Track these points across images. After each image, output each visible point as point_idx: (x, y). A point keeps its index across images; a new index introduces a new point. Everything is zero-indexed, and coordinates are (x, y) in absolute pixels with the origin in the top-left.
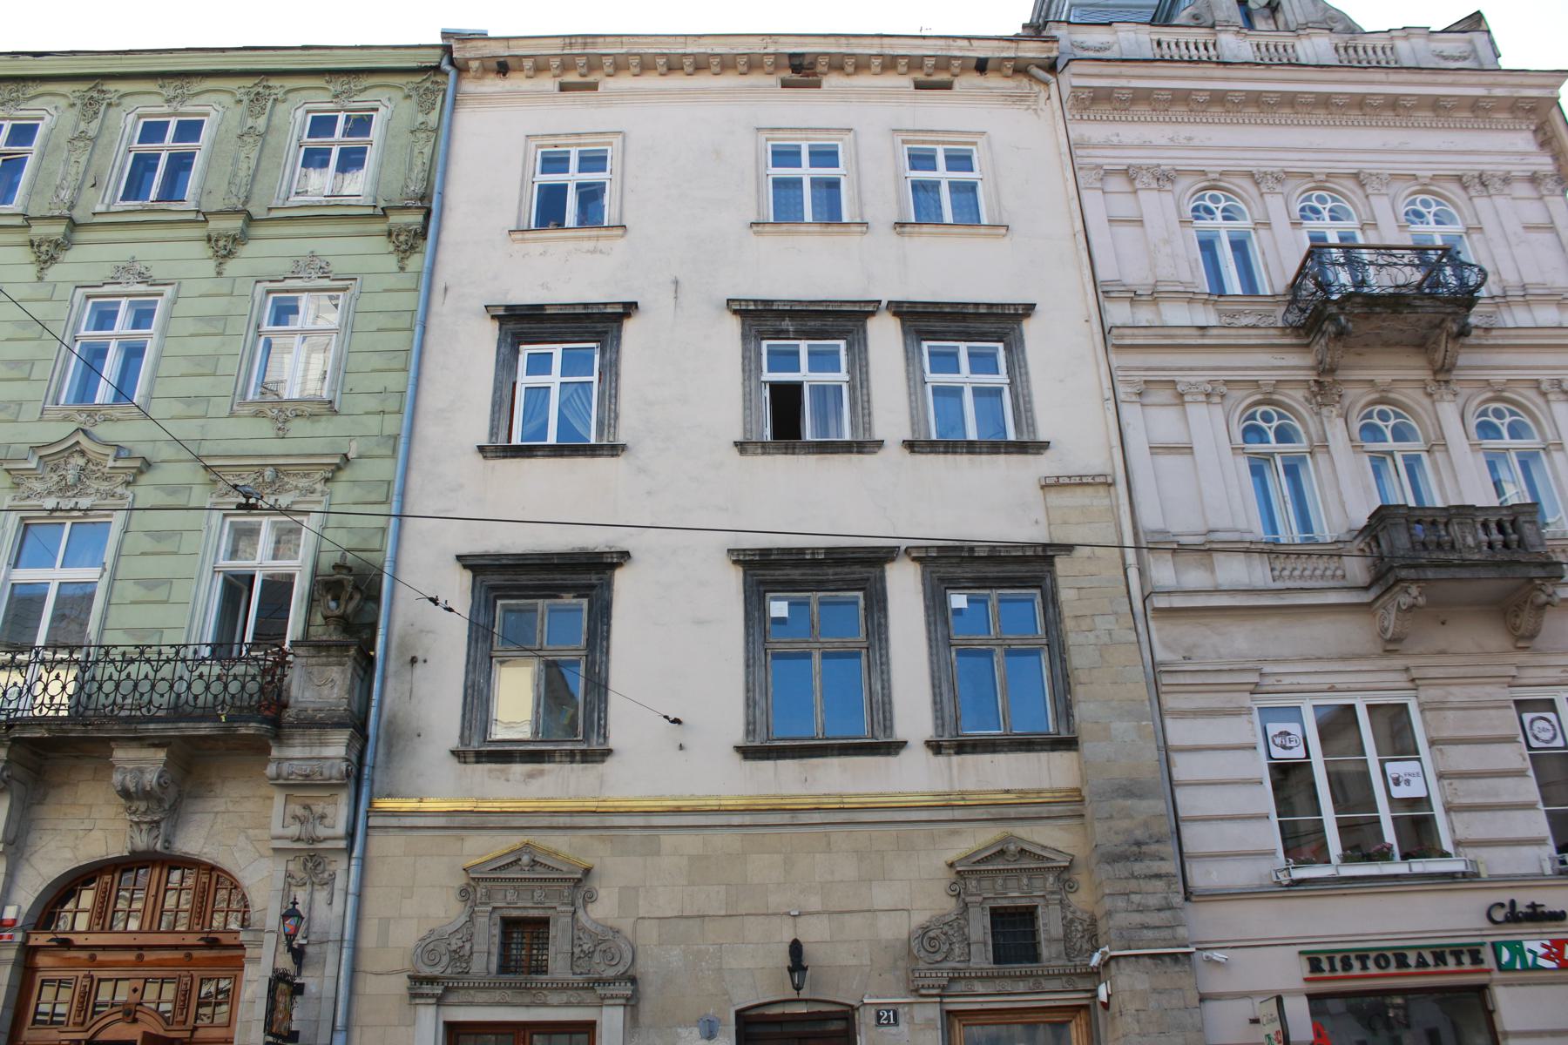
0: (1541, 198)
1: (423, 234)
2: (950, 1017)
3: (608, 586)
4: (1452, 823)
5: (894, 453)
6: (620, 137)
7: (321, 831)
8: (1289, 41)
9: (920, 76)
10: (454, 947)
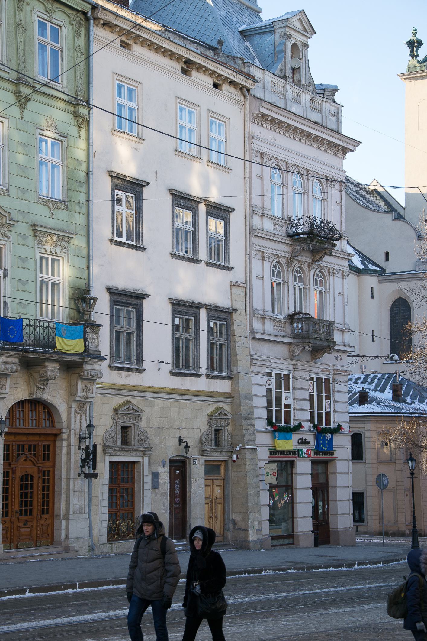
0: (340, 191)
1: (88, 122)
2: (205, 461)
3: (141, 305)
4: (295, 413)
5: (203, 264)
6: (141, 85)
7: (90, 395)
8: (300, 92)
9: (216, 81)
10: (112, 436)
